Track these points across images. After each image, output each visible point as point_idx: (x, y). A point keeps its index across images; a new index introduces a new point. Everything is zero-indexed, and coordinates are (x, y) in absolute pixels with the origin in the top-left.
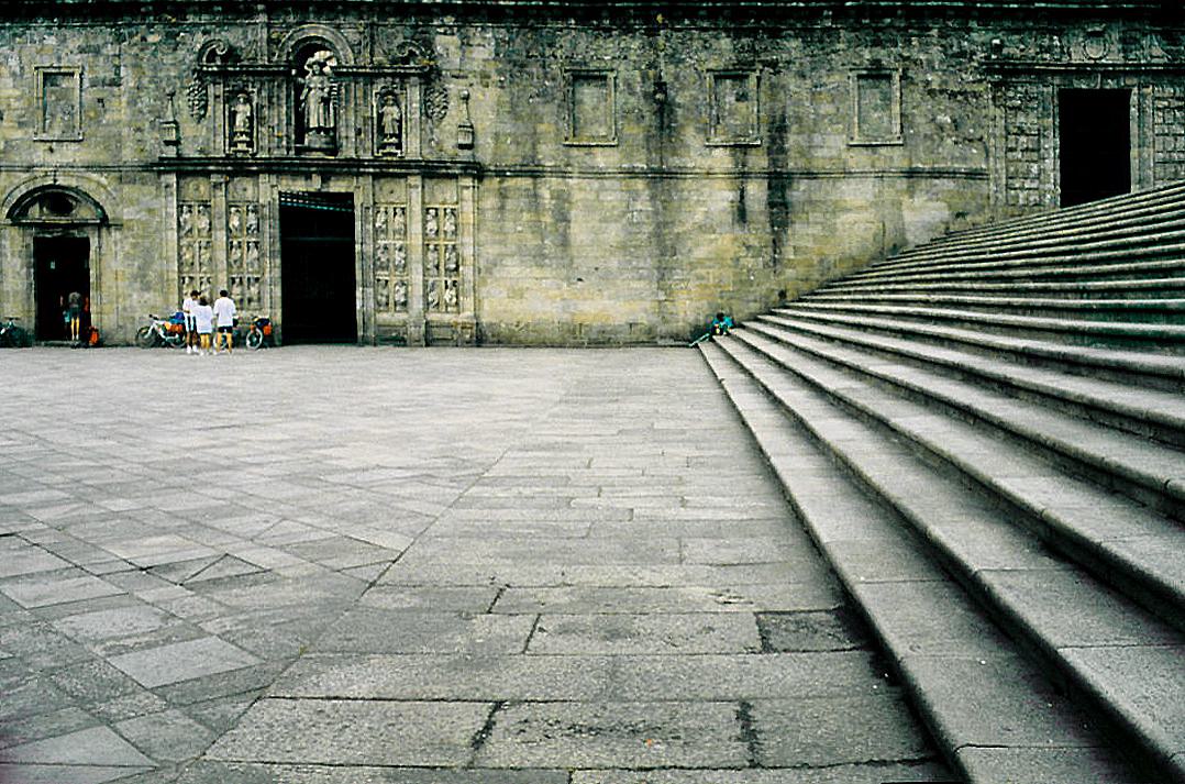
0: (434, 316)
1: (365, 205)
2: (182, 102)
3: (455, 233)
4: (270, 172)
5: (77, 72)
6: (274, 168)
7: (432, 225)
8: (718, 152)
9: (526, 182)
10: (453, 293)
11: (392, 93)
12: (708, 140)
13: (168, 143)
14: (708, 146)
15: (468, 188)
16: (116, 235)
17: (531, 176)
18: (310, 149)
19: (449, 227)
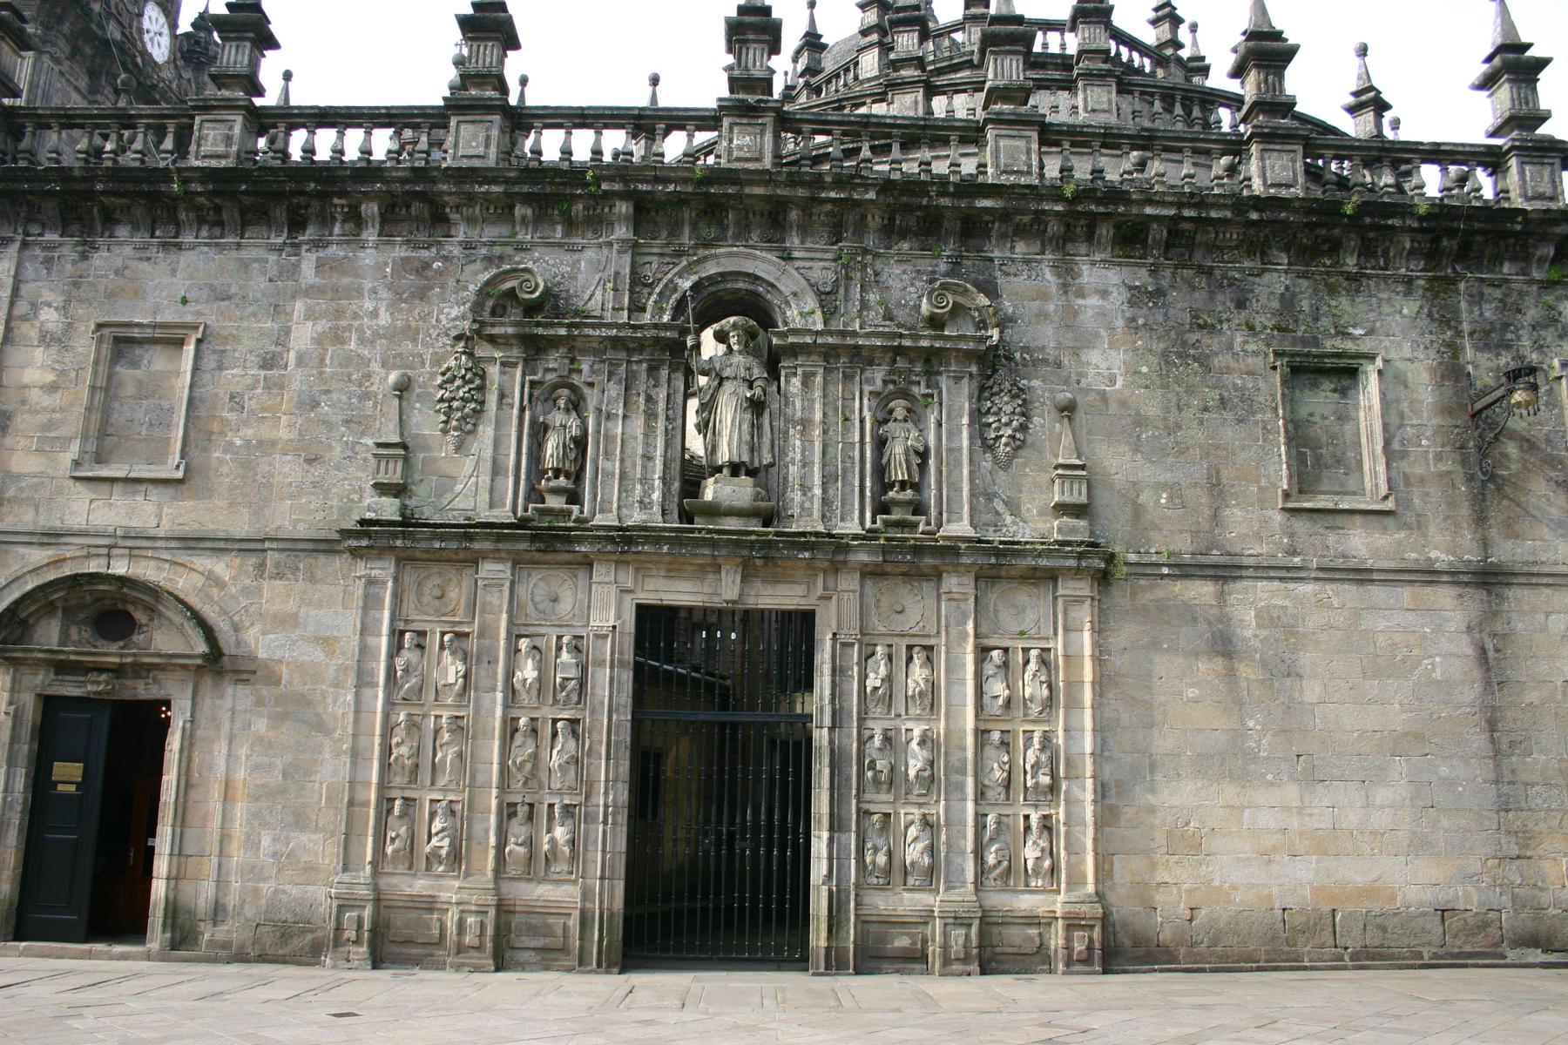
1: (842, 638)
9: (1201, 591)
10: (1043, 843)
11: (905, 394)
13: (382, 489)
16: (235, 697)
17: (1216, 578)
18: (713, 511)
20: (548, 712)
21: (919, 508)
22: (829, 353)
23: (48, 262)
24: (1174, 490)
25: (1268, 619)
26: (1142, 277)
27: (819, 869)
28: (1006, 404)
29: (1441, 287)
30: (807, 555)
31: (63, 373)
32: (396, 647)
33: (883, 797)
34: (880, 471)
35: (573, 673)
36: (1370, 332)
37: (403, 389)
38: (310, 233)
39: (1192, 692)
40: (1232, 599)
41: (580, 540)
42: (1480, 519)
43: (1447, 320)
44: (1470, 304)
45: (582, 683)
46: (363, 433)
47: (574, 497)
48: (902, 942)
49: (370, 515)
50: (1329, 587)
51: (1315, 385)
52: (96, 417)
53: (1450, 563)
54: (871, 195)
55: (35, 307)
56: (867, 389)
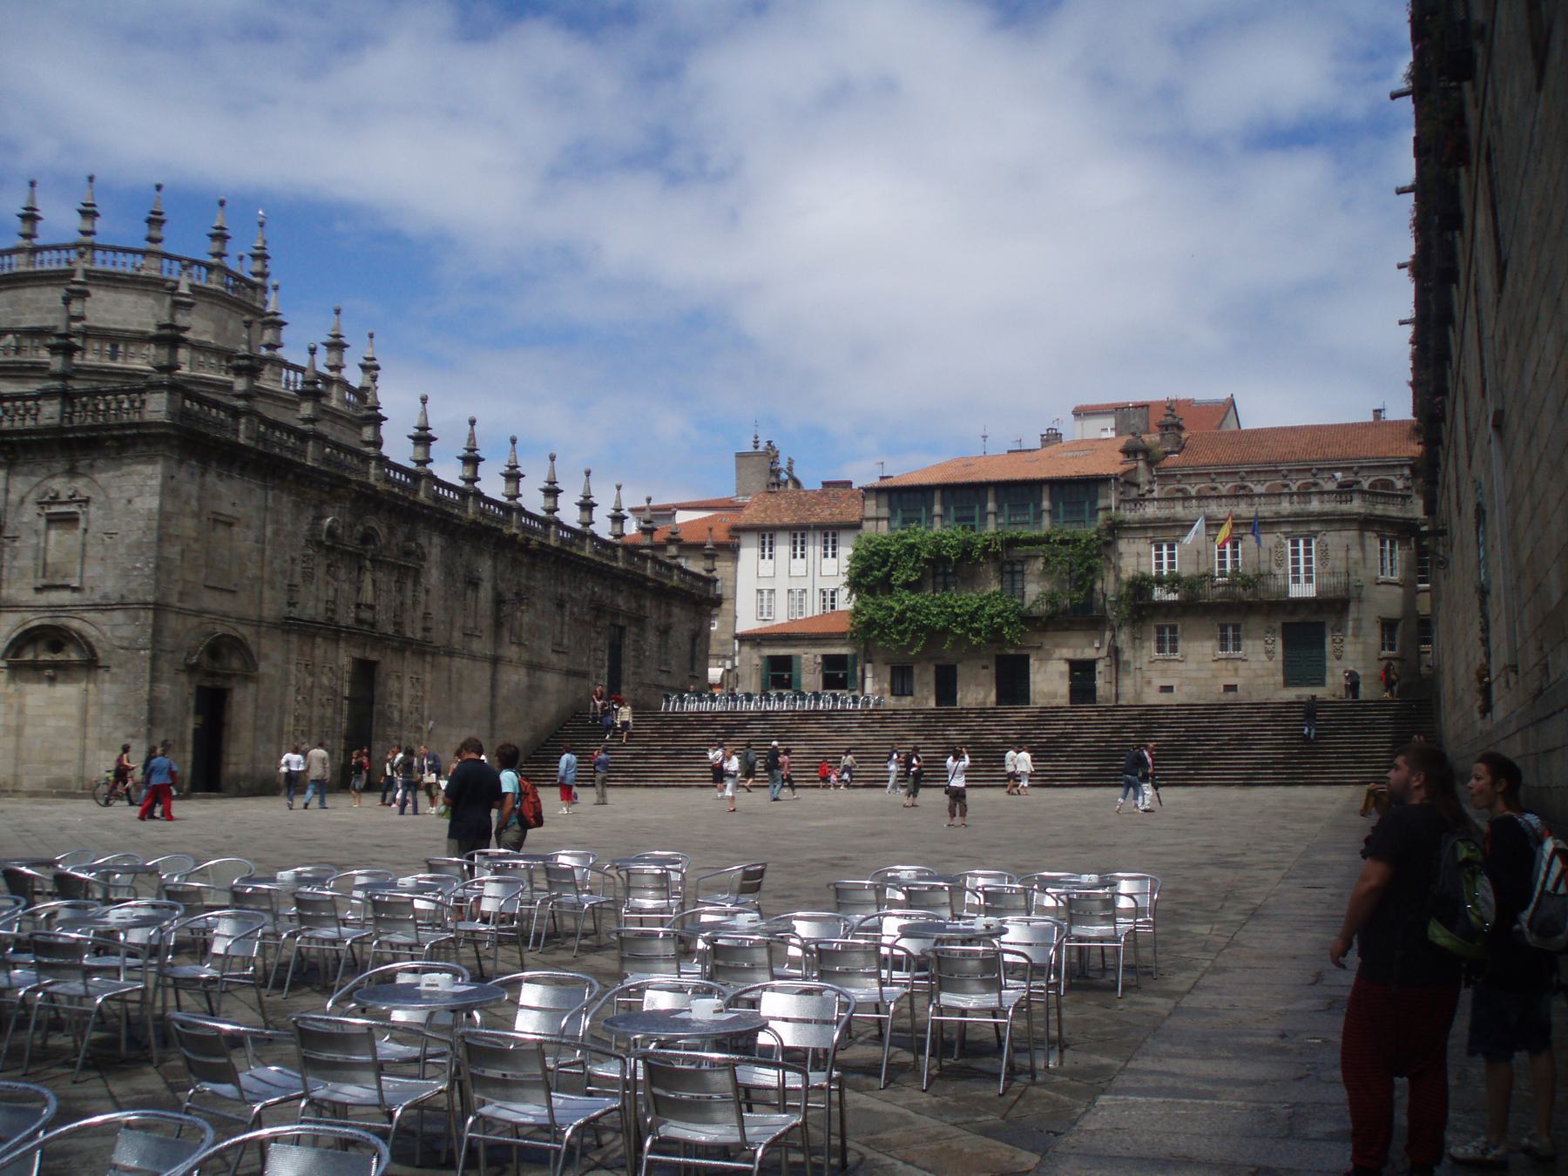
2: (298, 569)
16: (252, 687)
31: (199, 533)
37: (293, 560)
43: (495, 568)
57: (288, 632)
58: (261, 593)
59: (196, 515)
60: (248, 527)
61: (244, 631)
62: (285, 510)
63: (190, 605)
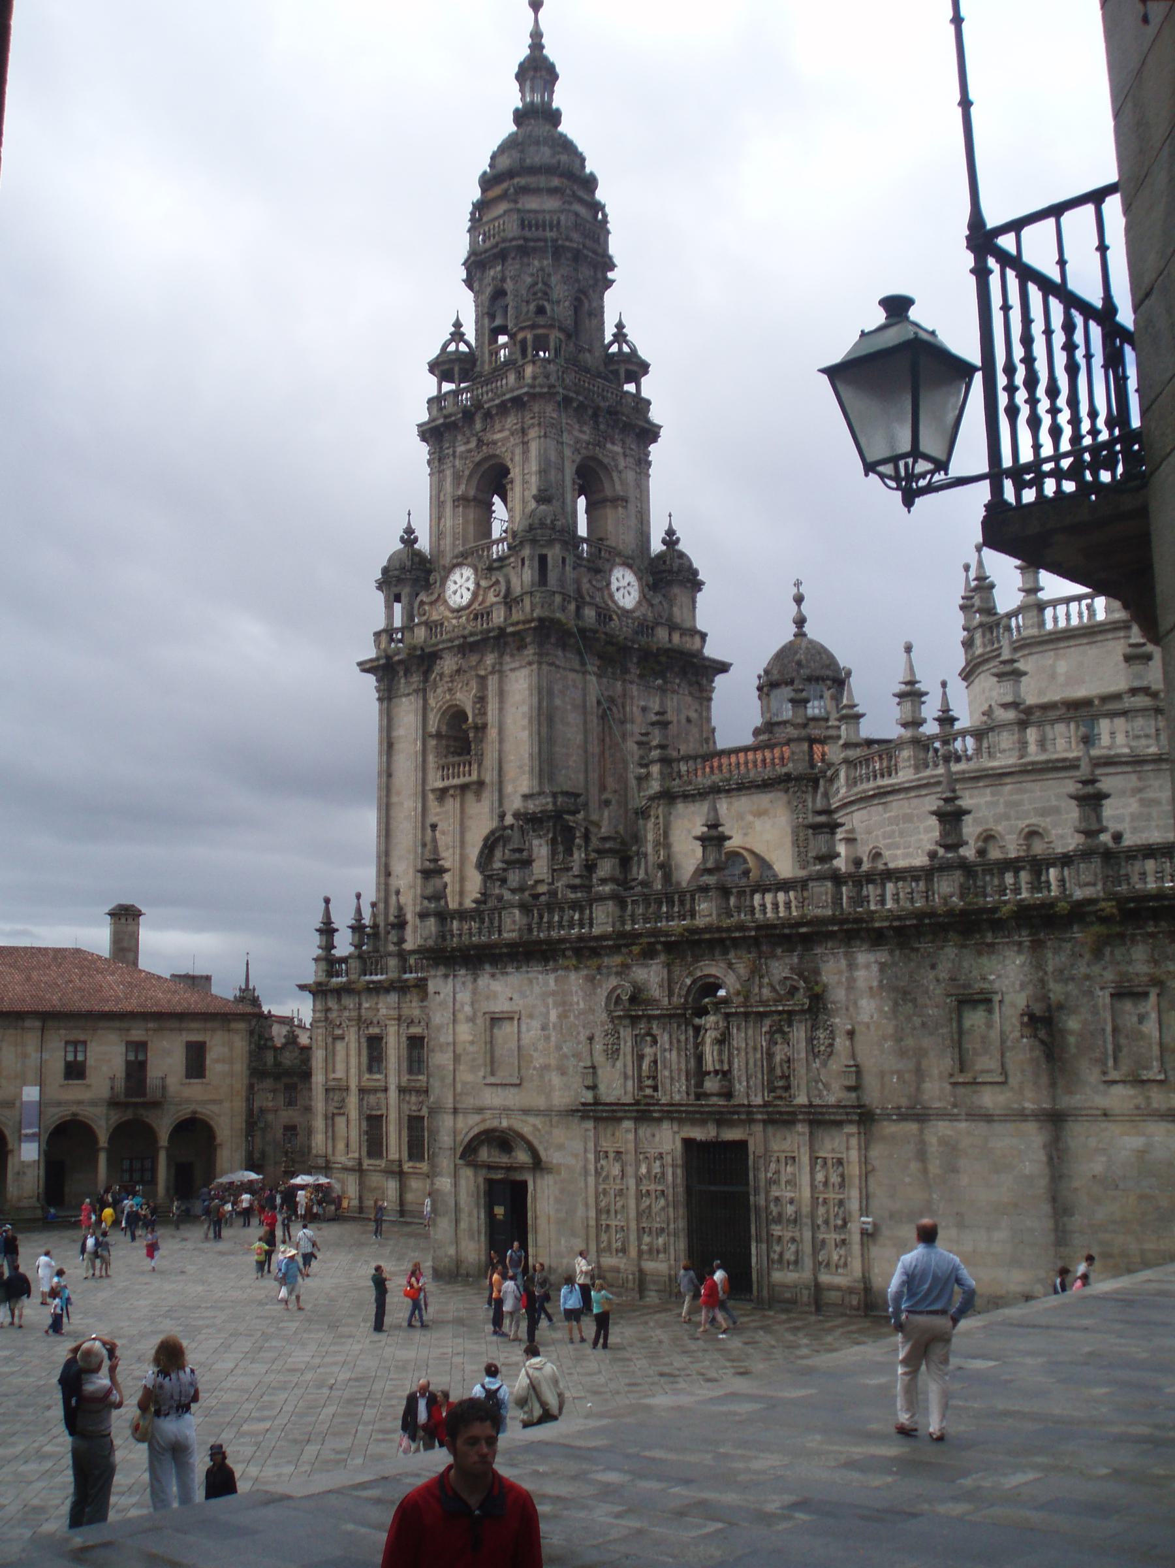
0: (825, 1278)
2: (598, 1047)
3: (842, 1185)
4: (672, 1119)
5: (517, 1017)
6: (673, 1114)
7: (820, 1177)
8: (1118, 1090)
9: (913, 1127)
12: (1104, 1073)
13: (588, 1088)
14: (1105, 1082)
15: (851, 1135)
17: (918, 1121)
18: (707, 1095)
19: (835, 1179)
20: (652, 1187)
21: (787, 1088)
22: (746, 1015)
23: (464, 983)
24: (900, 1073)
25: (943, 1142)
26: (883, 956)
27: (754, 1260)
28: (821, 1034)
29: (1037, 946)
30: (736, 1117)
31: (475, 1036)
32: (597, 1160)
33: (779, 1227)
34: (771, 1069)
35: (658, 1170)
36: (999, 976)
37: (591, 1039)
38: (551, 964)
39: (907, 1180)
40: (926, 1132)
41: (654, 1111)
42: (1053, 1085)
43: (1039, 966)
44: (1054, 954)
45: (663, 1173)
46: (580, 1060)
47: (655, 1089)
48: (788, 1295)
49: (583, 1100)
50: (973, 1125)
51: (974, 1009)
52: (488, 1056)
53: (1033, 1110)
54: (753, 933)
55: (462, 1006)
56: (764, 1030)
57: (583, 1118)
58: (550, 1081)
59: (472, 1019)
60: (531, 1016)
61: (526, 1126)
62: (574, 989)
63: (469, 1102)
